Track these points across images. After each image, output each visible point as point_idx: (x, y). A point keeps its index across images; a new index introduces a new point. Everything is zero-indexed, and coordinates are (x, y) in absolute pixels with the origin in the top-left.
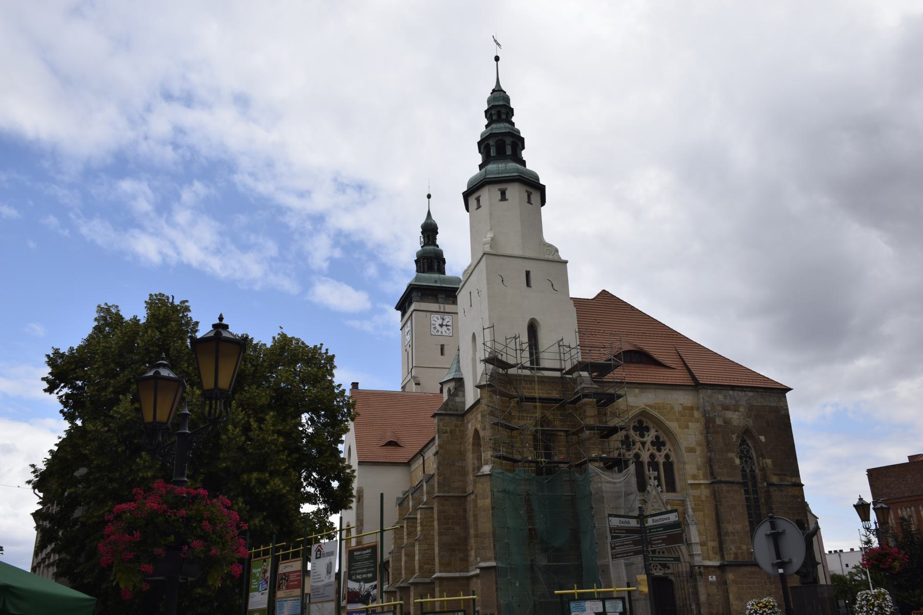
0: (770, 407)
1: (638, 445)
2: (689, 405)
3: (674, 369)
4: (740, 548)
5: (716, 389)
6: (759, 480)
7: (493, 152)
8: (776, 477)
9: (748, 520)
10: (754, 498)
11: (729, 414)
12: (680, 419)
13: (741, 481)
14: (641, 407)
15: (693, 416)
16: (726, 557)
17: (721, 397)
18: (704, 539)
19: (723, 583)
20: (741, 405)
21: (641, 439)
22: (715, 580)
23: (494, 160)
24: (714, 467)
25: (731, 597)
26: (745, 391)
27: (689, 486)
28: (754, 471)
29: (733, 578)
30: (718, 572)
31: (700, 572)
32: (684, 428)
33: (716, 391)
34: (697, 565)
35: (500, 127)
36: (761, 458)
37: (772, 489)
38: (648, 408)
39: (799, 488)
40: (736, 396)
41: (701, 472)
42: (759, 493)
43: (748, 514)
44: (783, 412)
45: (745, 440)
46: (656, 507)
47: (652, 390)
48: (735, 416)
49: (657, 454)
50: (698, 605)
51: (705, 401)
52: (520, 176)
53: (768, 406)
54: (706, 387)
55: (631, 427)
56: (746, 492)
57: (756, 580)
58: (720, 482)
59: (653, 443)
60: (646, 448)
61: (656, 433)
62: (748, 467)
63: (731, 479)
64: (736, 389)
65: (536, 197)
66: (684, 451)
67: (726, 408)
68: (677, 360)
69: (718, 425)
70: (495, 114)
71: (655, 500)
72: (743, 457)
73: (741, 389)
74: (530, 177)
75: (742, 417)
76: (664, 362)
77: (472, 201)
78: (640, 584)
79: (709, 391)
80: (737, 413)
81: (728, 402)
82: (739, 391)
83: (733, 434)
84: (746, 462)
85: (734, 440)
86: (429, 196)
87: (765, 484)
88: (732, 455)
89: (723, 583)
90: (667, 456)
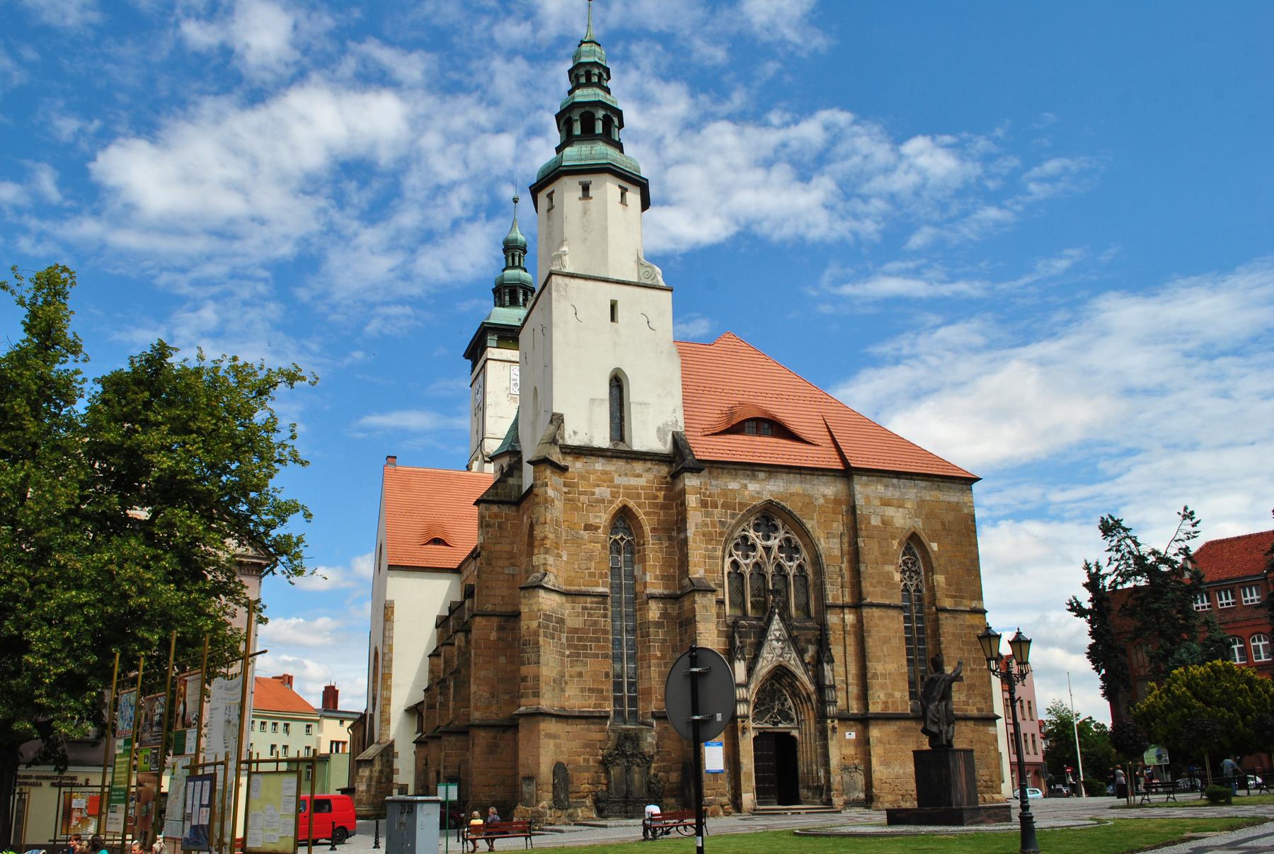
3: (818, 445)
4: (892, 695)
5: (876, 476)
6: (926, 604)
7: (577, 130)
9: (905, 658)
10: (918, 628)
11: (890, 512)
13: (901, 604)
17: (881, 488)
19: (864, 743)
21: (764, 543)
23: (577, 140)
25: (874, 761)
28: (920, 591)
31: (833, 726)
33: (875, 478)
36: (930, 574)
37: (942, 616)
39: (980, 615)
42: (926, 621)
43: (907, 649)
44: (966, 511)
45: (911, 548)
50: (828, 772)
52: (610, 164)
56: (907, 619)
58: (872, 605)
59: (780, 547)
63: (887, 602)
65: (634, 197)
67: (886, 503)
68: (823, 433)
76: (803, 436)
77: (542, 197)
80: (901, 510)
82: (906, 479)
83: (894, 539)
84: (911, 578)
87: (934, 608)
88: (891, 568)
89: (864, 743)
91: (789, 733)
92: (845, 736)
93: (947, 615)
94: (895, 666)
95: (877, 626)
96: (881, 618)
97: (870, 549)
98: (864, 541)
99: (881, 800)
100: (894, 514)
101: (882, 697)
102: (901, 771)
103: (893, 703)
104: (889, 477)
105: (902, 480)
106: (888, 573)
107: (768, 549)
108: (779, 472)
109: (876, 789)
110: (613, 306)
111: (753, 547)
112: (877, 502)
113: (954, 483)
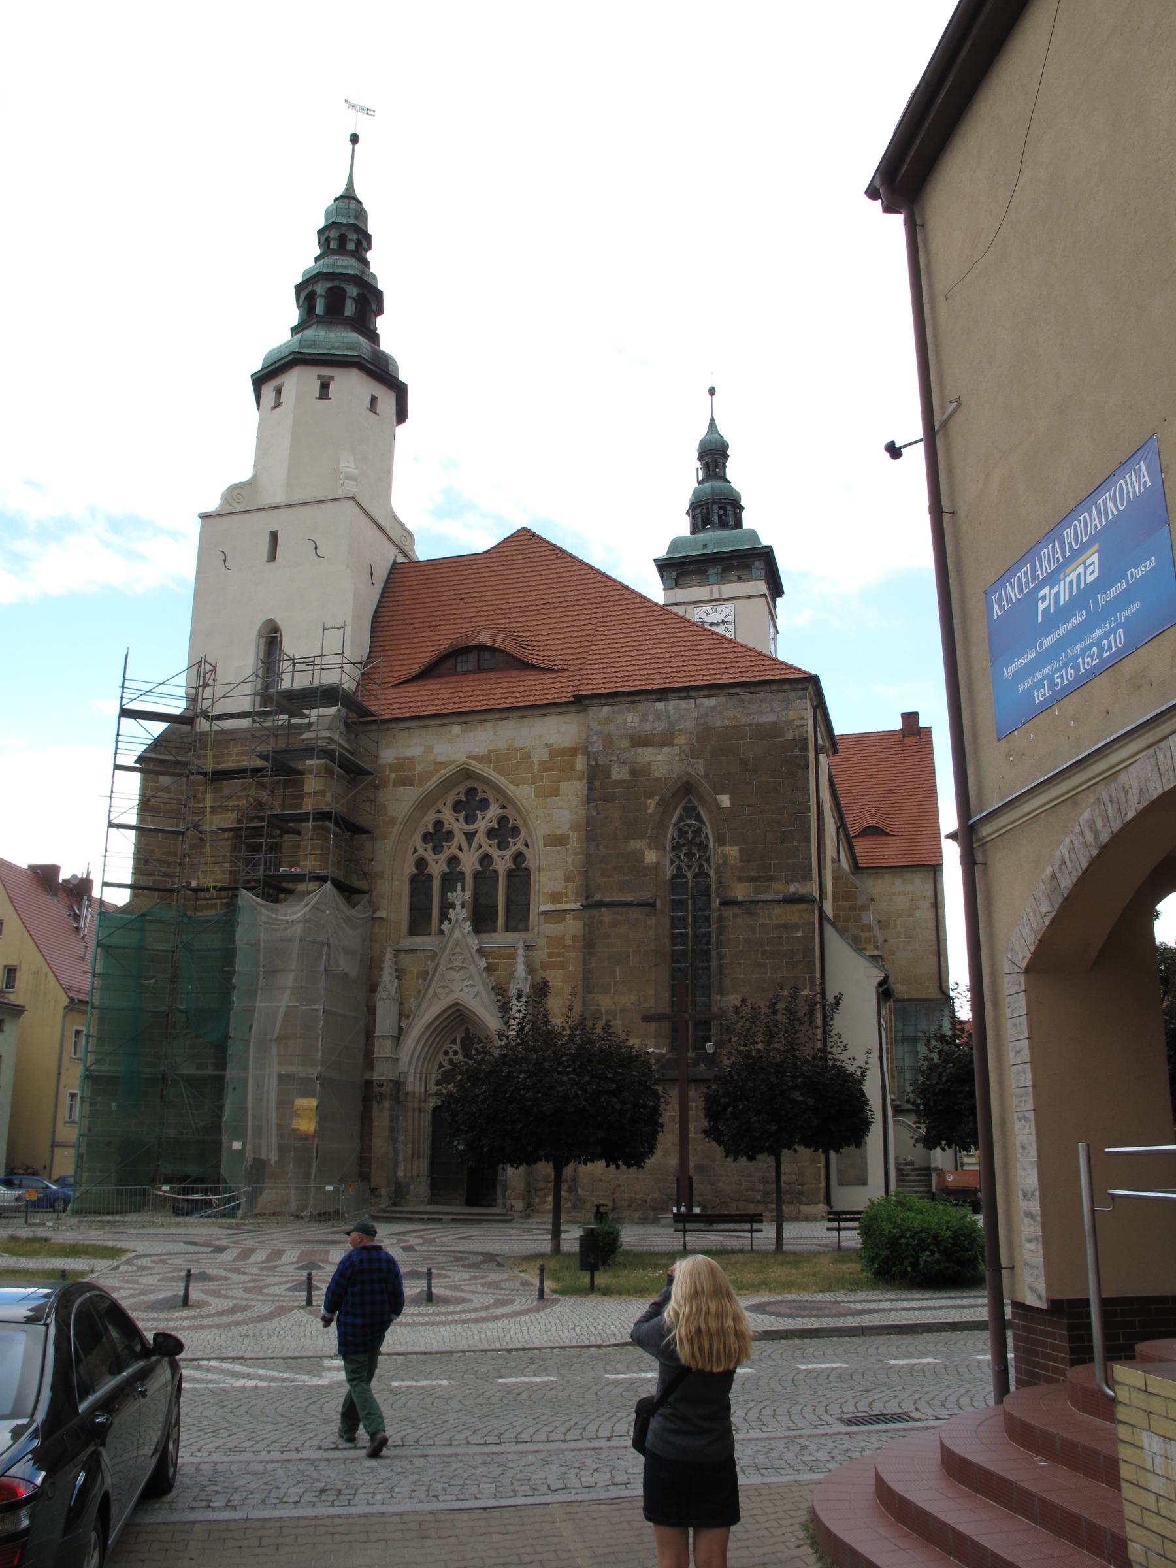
0: (758, 725)
1: (459, 838)
2: (567, 744)
3: (559, 670)
5: (625, 703)
8: (745, 884)
11: (647, 755)
12: (542, 777)
14: (458, 763)
15: (573, 768)
20: (682, 730)
26: (695, 698)
27: (542, 918)
35: (347, 265)
37: (730, 912)
38: (473, 762)
40: (672, 712)
41: (572, 886)
44: (790, 734)
45: (694, 808)
46: (457, 963)
47: (489, 725)
48: (660, 757)
49: (495, 853)
51: (592, 733)
53: (750, 725)
54: (595, 701)
55: (450, 803)
58: (600, 904)
60: (475, 844)
61: (500, 811)
62: (690, 867)
63: (629, 898)
64: (671, 696)
67: (640, 741)
69: (616, 781)
70: (334, 239)
71: (457, 950)
72: (684, 845)
73: (684, 694)
74: (333, 348)
75: (677, 758)
78: (298, 1116)
79: (606, 709)
80: (666, 749)
81: (647, 727)
82: (680, 698)
84: (690, 855)
85: (650, 811)
86: (712, 391)
90: (518, 857)
93: (736, 910)
100: (653, 758)
104: (648, 701)
105: (672, 702)
107: (470, 836)
108: (480, 721)
110: (274, 535)
111: (450, 835)
112: (625, 744)
113: (771, 691)
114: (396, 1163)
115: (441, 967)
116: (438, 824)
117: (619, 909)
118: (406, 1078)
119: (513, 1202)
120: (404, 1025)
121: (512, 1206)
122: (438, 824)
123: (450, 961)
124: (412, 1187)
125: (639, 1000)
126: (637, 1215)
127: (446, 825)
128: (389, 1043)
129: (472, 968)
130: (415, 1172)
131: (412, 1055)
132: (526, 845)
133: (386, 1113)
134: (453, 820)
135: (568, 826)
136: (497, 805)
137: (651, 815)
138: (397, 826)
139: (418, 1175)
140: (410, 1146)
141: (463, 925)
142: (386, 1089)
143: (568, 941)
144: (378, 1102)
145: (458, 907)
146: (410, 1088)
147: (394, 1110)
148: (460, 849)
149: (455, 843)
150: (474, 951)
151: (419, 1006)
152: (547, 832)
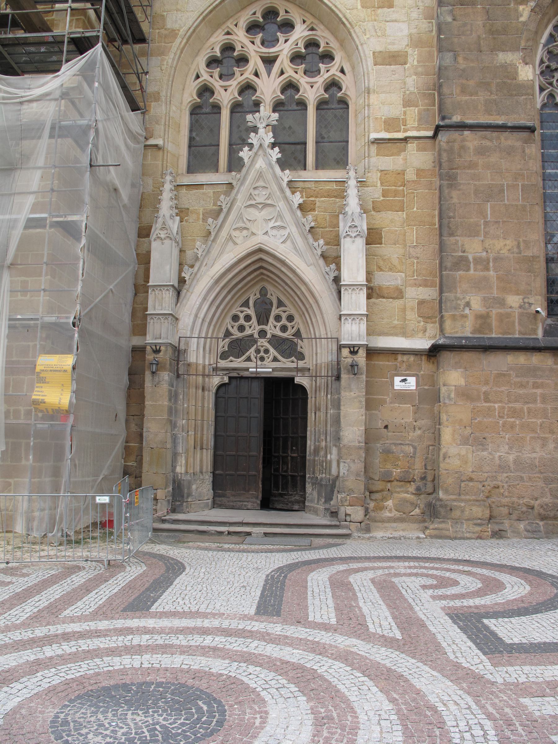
1: (255, 62)
4: (501, 303)
16: (448, 324)
18: (399, 282)
22: (414, 388)
24: (445, 90)
25: (447, 434)
27: (374, 148)
29: (462, 382)
30: (426, 367)
32: (378, 8)
34: (349, 346)
57: (539, 391)
58: (462, 127)
61: (307, 33)
66: (370, 61)
71: (261, 183)
78: (43, 381)
85: (522, 19)
91: (293, 379)
92: (393, 384)
94: (510, 243)
95: (472, 165)
96: (481, 151)
97: (465, 25)
98: (451, 11)
99: (456, 514)
101: (477, 304)
102: (511, 458)
103: (501, 318)
106: (504, 67)
109: (446, 491)
111: (243, 60)
114: (175, 455)
115: (238, 204)
116: (228, 48)
117: (488, 133)
118: (187, 344)
119: (349, 510)
120: (186, 275)
121: (346, 515)
122: (228, 48)
123: (251, 197)
124: (194, 487)
125: (518, 246)
126: (522, 526)
127: (238, 48)
128: (168, 296)
129: (282, 205)
130: (198, 469)
131: (196, 316)
132: (342, 71)
133: (165, 387)
134: (247, 42)
135: (405, 42)
136: (305, 26)
137: (524, 23)
138: (178, 40)
139: (201, 472)
140: (191, 433)
141: (271, 151)
142: (165, 356)
143: (410, 175)
144: (153, 373)
145: (261, 131)
146: (192, 358)
147: (172, 386)
148: (256, 74)
149: (251, 67)
150: (284, 184)
151: (208, 252)
152: (378, 49)
